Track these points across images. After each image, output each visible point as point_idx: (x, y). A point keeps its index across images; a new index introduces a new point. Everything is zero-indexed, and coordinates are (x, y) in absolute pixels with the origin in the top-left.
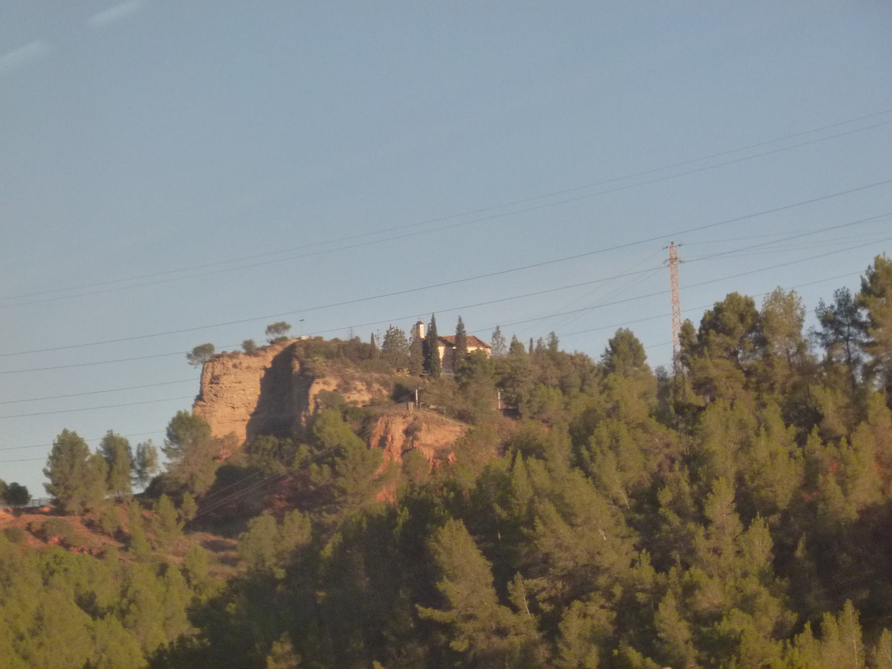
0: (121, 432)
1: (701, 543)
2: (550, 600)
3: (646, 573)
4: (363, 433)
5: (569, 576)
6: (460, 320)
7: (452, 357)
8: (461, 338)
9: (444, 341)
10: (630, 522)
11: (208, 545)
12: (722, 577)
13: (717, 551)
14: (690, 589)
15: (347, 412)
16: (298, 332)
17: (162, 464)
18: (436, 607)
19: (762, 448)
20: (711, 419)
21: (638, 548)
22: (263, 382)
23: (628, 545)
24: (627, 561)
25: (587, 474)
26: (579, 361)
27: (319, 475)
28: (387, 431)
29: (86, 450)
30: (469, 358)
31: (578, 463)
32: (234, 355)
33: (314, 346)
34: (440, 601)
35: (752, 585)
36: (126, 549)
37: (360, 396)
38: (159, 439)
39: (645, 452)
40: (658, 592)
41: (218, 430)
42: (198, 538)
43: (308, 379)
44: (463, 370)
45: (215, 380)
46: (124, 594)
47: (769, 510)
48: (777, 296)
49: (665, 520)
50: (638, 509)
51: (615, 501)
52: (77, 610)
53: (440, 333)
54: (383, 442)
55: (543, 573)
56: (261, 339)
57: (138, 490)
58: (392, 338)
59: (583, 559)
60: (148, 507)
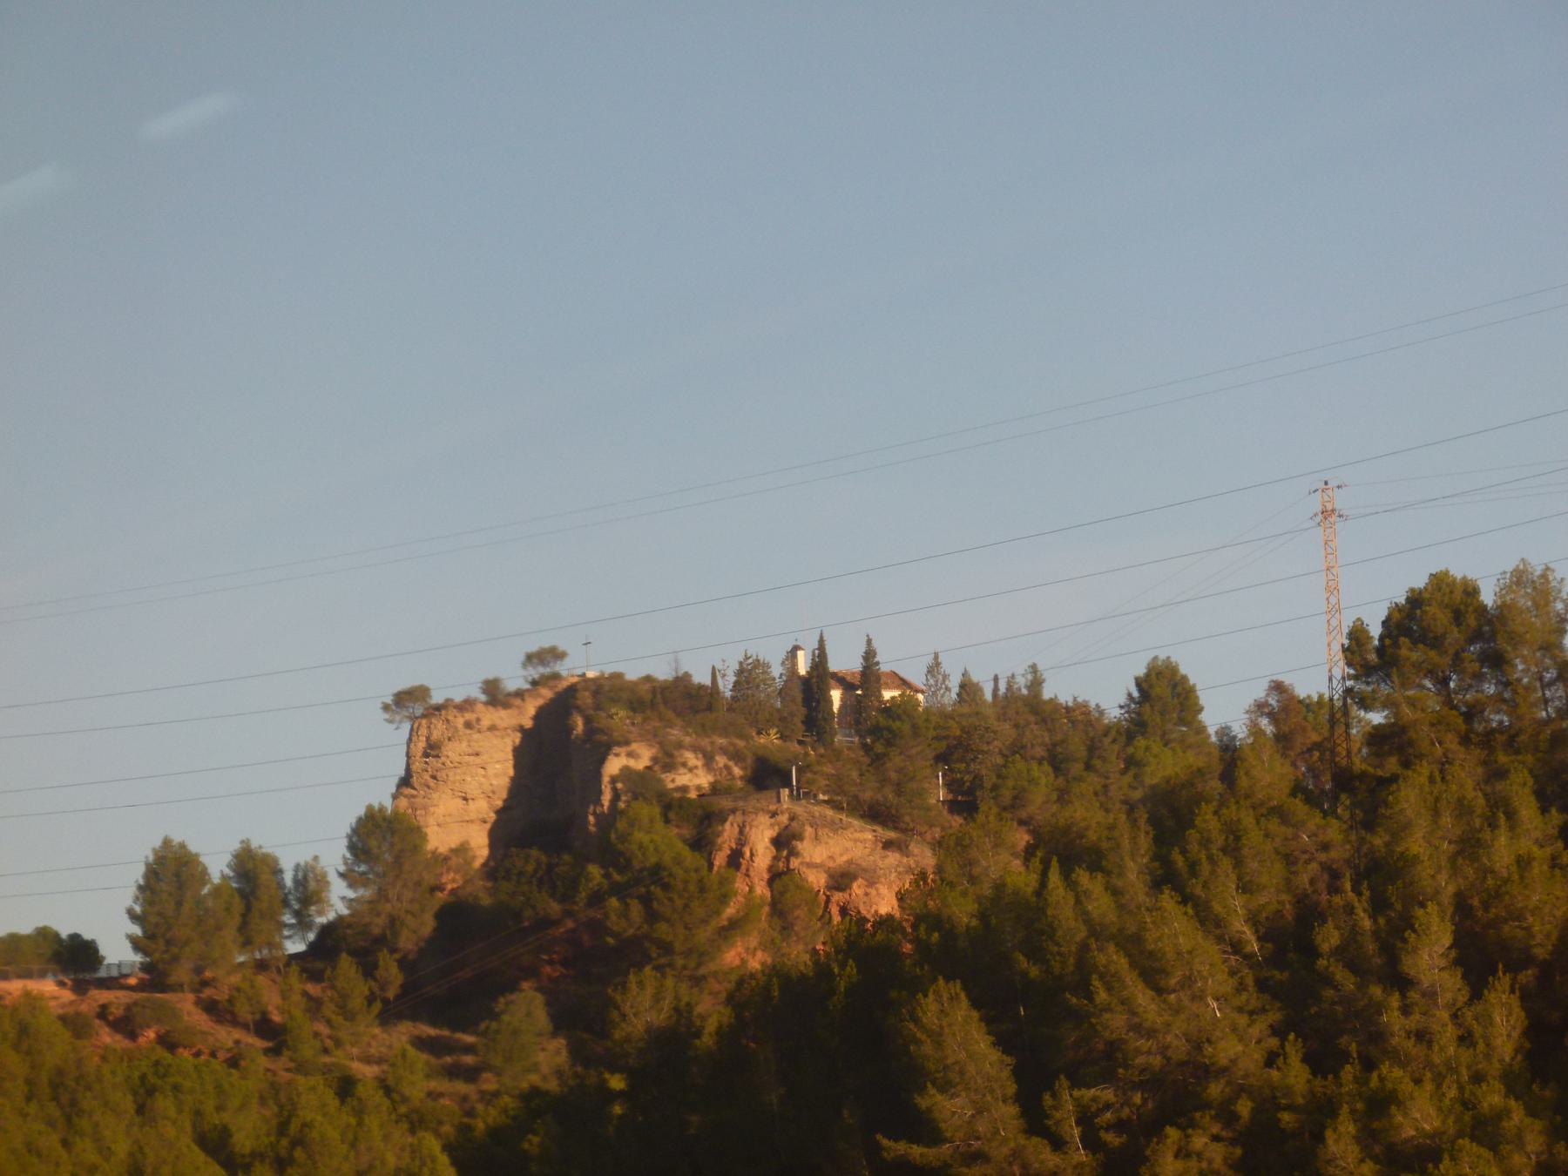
0: (266, 841)
1: (1393, 1019)
2: (1119, 1126)
3: (1296, 1075)
4: (702, 843)
5: (1151, 1082)
6: (869, 642)
7: (855, 708)
8: (870, 675)
9: (841, 681)
10: (1262, 985)
11: (421, 1043)
12: (1439, 1080)
13: (1422, 1036)
14: (1380, 1104)
15: (672, 806)
16: (582, 664)
17: (338, 899)
18: (913, 1140)
19: (1502, 850)
20: (1409, 798)
21: (1277, 1031)
22: (518, 752)
23: (1259, 1028)
24: (1258, 1055)
25: (1185, 899)
26: (1080, 716)
27: (623, 918)
28: (742, 840)
29: (204, 874)
30: (889, 710)
31: (1165, 878)
32: (466, 705)
33: (609, 690)
34: (924, 1129)
35: (1493, 1097)
36: (275, 1052)
37: (693, 778)
38: (333, 856)
39: (1289, 860)
40: (1322, 1112)
41: (439, 839)
42: (401, 1035)
43: (600, 747)
44: (876, 731)
45: (433, 749)
46: (282, 1129)
47: (1518, 960)
48: (1519, 578)
49: (1327, 980)
50: (1276, 959)
51: (1236, 947)
52: (199, 1156)
53: (834, 666)
54: (735, 859)
55: (1107, 1077)
56: (515, 679)
57: (295, 946)
58: (749, 674)
59: (1179, 1048)
60: (315, 976)
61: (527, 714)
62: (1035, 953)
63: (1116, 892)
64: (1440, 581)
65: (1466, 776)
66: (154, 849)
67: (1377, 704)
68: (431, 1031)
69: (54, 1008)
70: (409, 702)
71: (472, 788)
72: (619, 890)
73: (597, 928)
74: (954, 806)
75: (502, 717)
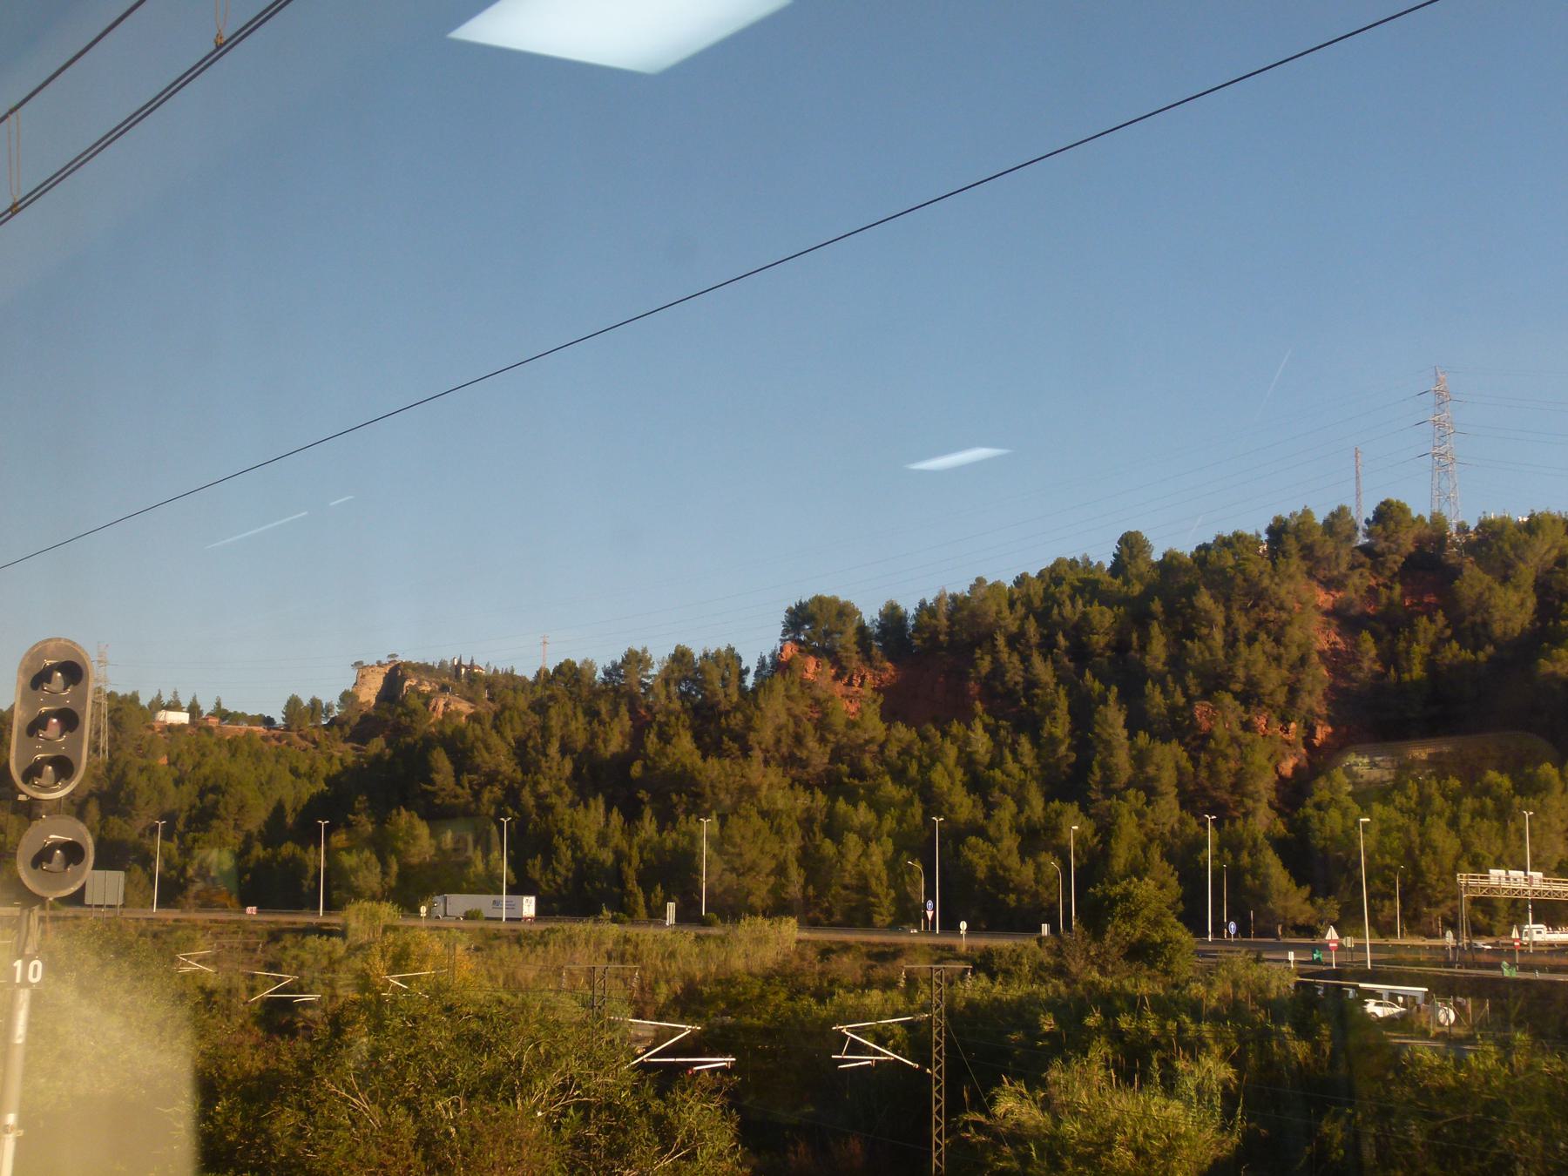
0: (319, 697)
1: (543, 764)
2: (478, 784)
3: (519, 776)
4: (426, 704)
5: (486, 775)
7: (468, 673)
8: (472, 666)
9: (465, 666)
10: (515, 754)
11: (353, 748)
12: (550, 779)
13: (550, 768)
14: (536, 783)
15: (420, 694)
16: (402, 658)
17: (336, 712)
18: (429, 784)
19: (573, 726)
20: (553, 712)
21: (516, 765)
22: (384, 678)
23: (513, 763)
24: (511, 770)
25: (498, 732)
26: (523, 679)
27: (405, 720)
28: (436, 704)
29: (301, 704)
30: (475, 674)
31: (495, 727)
32: (372, 666)
33: (408, 665)
34: (431, 782)
35: (563, 784)
36: (316, 748)
37: (426, 688)
38: (336, 701)
39: (524, 724)
40: (523, 784)
41: (362, 699)
42: (348, 746)
43: (404, 678)
44: (471, 680)
45: (363, 676)
46: (311, 768)
47: (573, 751)
48: (585, 662)
49: (529, 753)
50: (518, 748)
51: (509, 744)
52: (288, 773)
53: (463, 663)
54: (434, 709)
55: (476, 773)
56: (385, 660)
57: (324, 722)
58: (442, 664)
59: (492, 766)
60: (328, 730)
61: (387, 669)
62: (462, 743)
63: (483, 729)
64: (567, 661)
65: (568, 709)
66: (923, 604)
67: (790, 650)
68: (356, 745)
69: (258, 735)
70: (358, 665)
71: (372, 686)
72: (405, 715)
73: (399, 723)
74: (489, 699)
75: (382, 670)
